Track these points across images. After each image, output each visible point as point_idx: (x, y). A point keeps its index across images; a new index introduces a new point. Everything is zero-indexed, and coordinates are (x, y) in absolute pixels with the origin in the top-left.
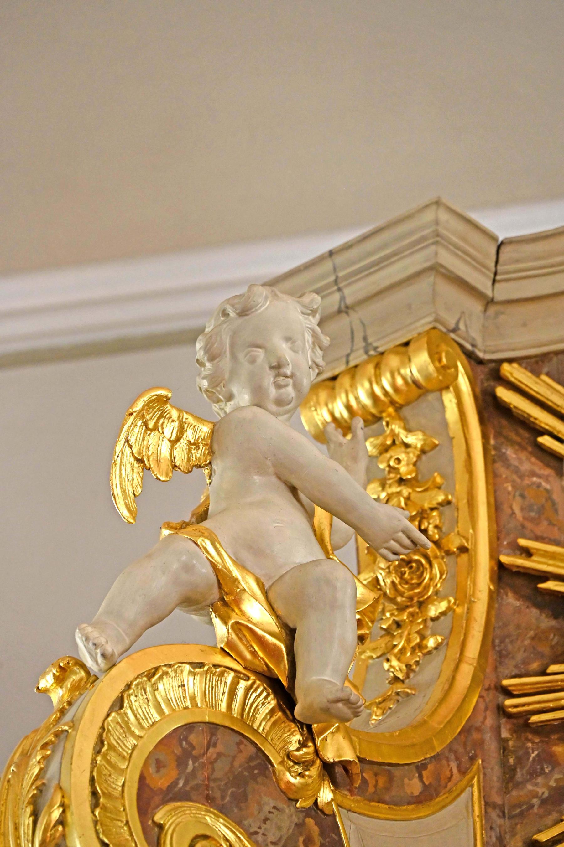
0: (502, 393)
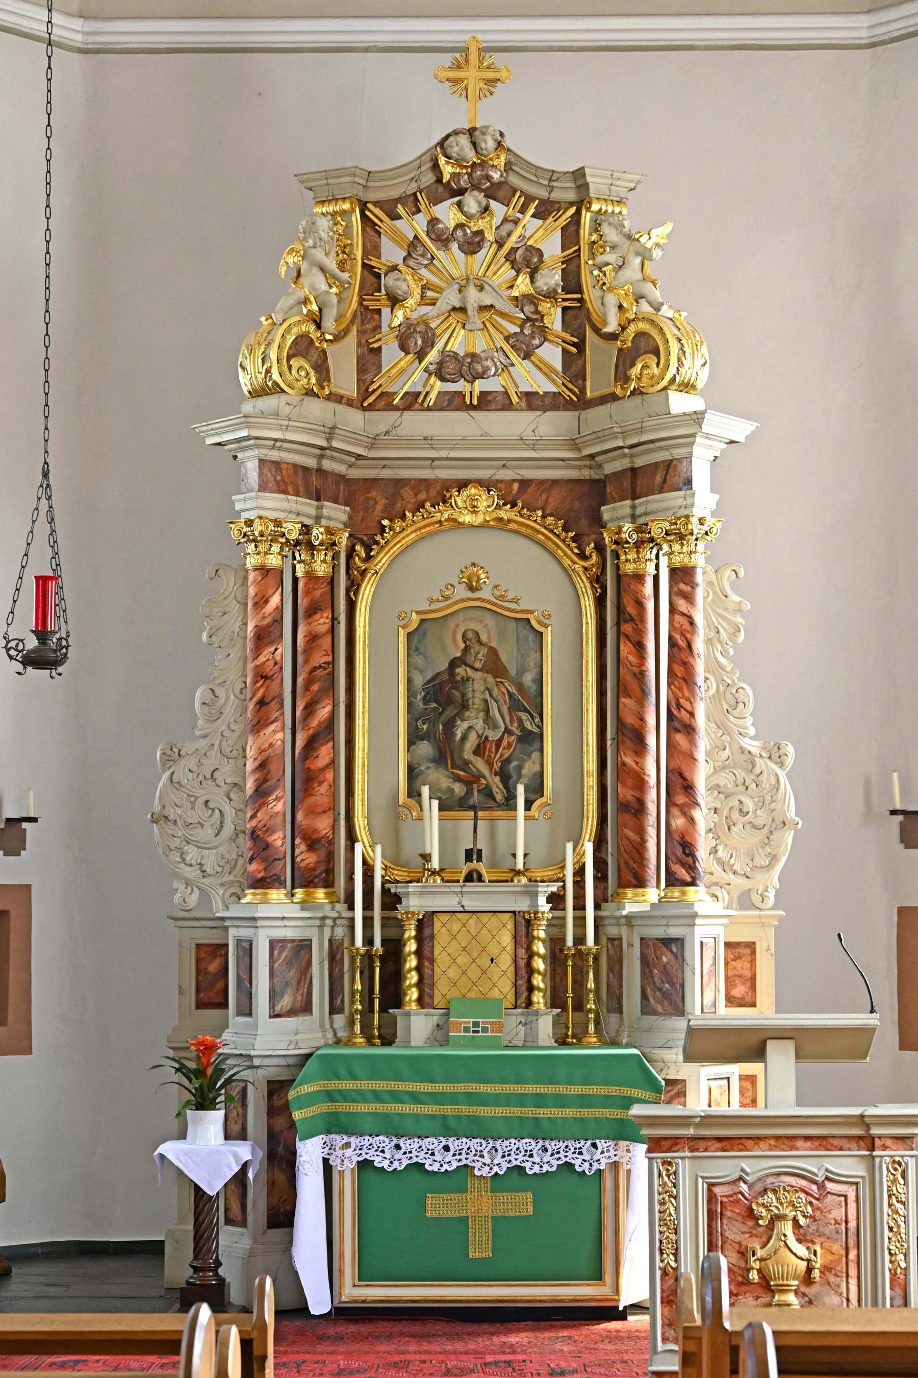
0: (367, 213)
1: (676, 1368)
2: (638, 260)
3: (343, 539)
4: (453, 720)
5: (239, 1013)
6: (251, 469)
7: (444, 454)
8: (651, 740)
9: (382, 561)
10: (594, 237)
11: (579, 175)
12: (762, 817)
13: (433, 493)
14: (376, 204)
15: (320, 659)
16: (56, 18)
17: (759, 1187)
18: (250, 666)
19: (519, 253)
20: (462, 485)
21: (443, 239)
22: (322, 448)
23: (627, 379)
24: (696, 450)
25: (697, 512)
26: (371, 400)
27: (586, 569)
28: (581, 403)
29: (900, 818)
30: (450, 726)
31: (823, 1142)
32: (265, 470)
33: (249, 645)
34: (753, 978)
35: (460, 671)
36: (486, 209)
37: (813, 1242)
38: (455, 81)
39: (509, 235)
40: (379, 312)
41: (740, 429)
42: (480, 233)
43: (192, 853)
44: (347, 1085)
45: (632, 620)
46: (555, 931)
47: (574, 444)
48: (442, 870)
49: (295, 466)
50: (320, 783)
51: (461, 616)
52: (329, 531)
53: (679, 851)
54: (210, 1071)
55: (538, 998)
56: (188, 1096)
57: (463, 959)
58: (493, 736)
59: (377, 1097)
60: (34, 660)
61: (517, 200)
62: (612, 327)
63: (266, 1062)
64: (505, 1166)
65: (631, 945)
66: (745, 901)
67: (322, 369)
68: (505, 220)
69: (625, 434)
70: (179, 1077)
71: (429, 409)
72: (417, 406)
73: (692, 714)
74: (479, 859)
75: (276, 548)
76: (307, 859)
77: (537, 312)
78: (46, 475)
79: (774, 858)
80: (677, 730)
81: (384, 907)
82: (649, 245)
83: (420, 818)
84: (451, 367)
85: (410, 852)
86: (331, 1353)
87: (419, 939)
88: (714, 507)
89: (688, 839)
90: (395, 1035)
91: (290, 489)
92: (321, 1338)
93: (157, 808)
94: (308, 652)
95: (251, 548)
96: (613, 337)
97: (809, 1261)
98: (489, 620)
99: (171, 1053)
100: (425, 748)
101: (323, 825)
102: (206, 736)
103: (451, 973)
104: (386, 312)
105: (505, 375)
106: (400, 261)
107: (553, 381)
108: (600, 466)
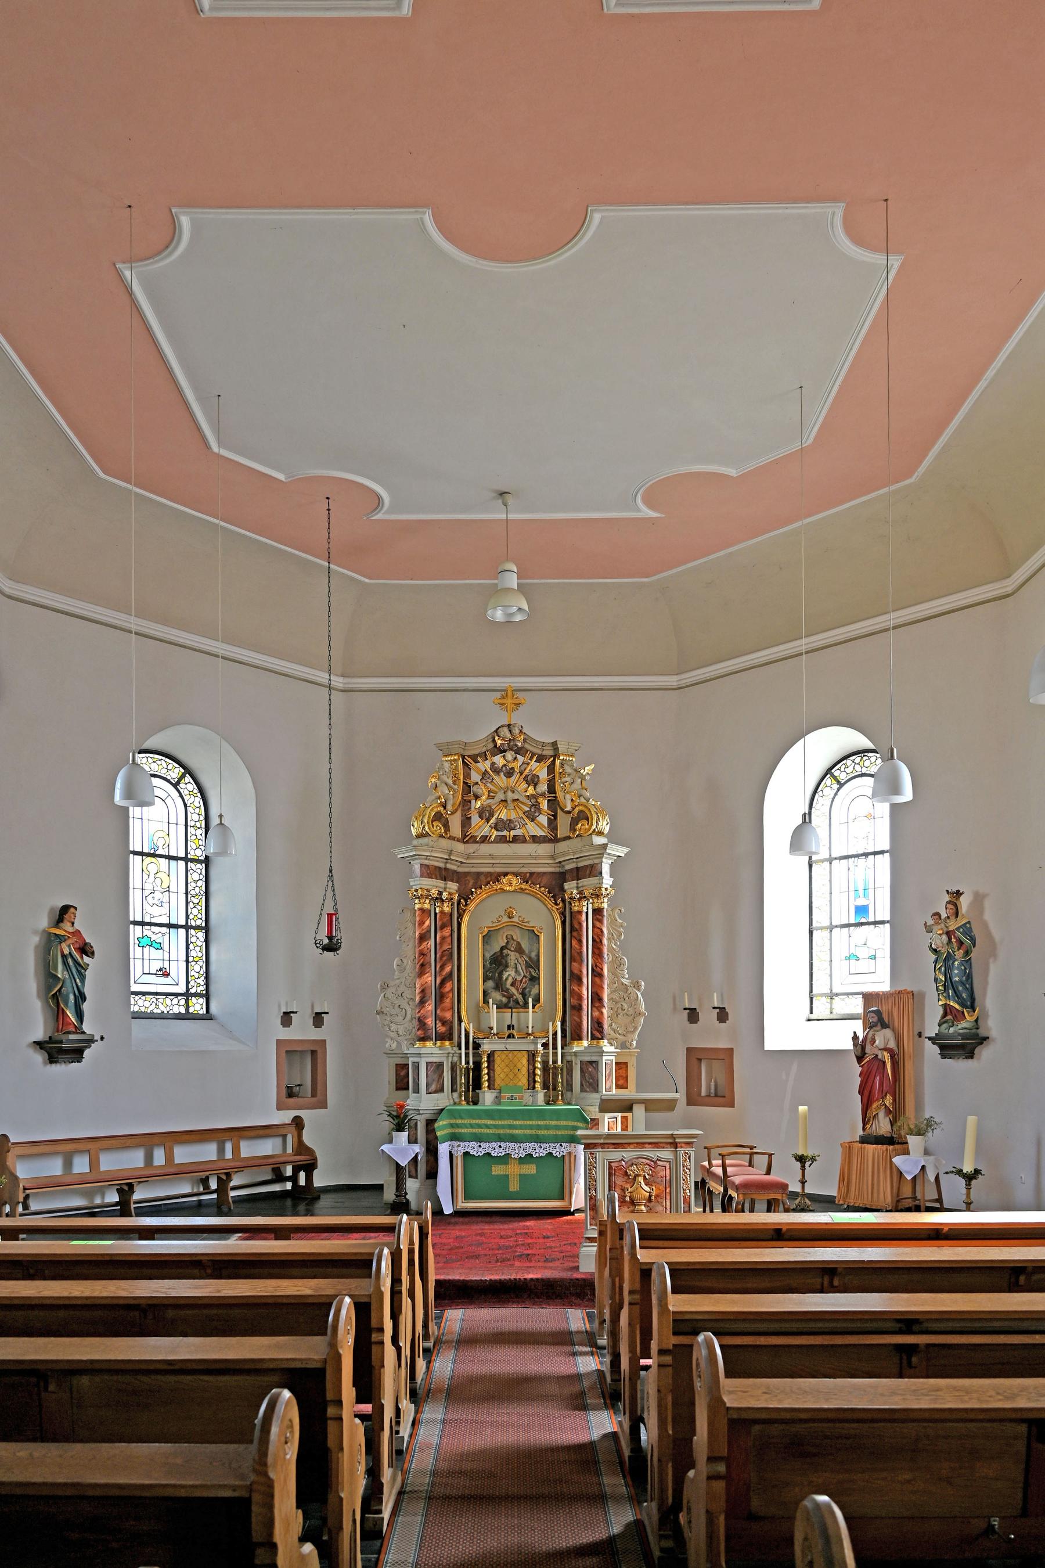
1: (596, 1236)
2: (580, 780)
3: (456, 897)
4: (502, 971)
5: (414, 1092)
6: (417, 868)
7: (498, 862)
8: (585, 980)
9: (472, 906)
10: (561, 771)
11: (554, 745)
12: (631, 1011)
13: (493, 878)
14: (468, 756)
15: (446, 947)
16: (333, 677)
17: (630, 1163)
18: (417, 950)
19: (529, 777)
20: (506, 874)
21: (497, 771)
22: (447, 859)
23: (575, 830)
24: (604, 860)
25: (604, 886)
26: (467, 839)
27: (557, 909)
28: (555, 840)
29: (688, 1011)
30: (501, 974)
31: (656, 1145)
32: (423, 869)
33: (417, 942)
34: (627, 1077)
35: (505, 951)
36: (515, 758)
37: (652, 1185)
38: (502, 704)
39: (525, 770)
40: (470, 802)
41: (621, 851)
42: (513, 768)
43: (393, 1027)
44: (459, 1121)
45: (577, 930)
46: (544, 1058)
47: (552, 857)
48: (497, 1033)
49: (435, 867)
50: (447, 998)
51: (505, 928)
52: (450, 894)
53: (596, 1025)
54: (402, 1116)
55: (538, 1085)
56: (393, 1126)
57: (506, 1070)
58: (519, 978)
59: (471, 1126)
60: (327, 948)
61: (529, 755)
62: (568, 808)
63: (425, 1112)
64: (524, 1154)
65: (576, 1064)
66: (623, 1046)
67: (446, 826)
68: (523, 763)
69: (574, 853)
70: (389, 1118)
71: (491, 843)
72: (486, 841)
73: (602, 969)
74: (513, 1029)
75: (427, 901)
76: (442, 1029)
77: (537, 802)
78: (331, 871)
79: (636, 1028)
80: (595, 976)
81: (473, 1049)
82: (584, 774)
83: (489, 1012)
84: (501, 825)
85: (484, 1026)
86: (453, 1230)
87: (488, 1062)
88: (611, 883)
89: (600, 1020)
90: (478, 1101)
91: (434, 877)
92: (449, 1224)
93: (379, 1008)
94: (441, 944)
95: (417, 901)
96: (569, 812)
97: (650, 1193)
98: (518, 931)
99: (385, 1109)
100: (490, 984)
101: (448, 1015)
102: (399, 979)
103: (501, 1075)
104: (473, 802)
105: (524, 828)
106: (479, 781)
107: (543, 831)
108: (563, 866)
